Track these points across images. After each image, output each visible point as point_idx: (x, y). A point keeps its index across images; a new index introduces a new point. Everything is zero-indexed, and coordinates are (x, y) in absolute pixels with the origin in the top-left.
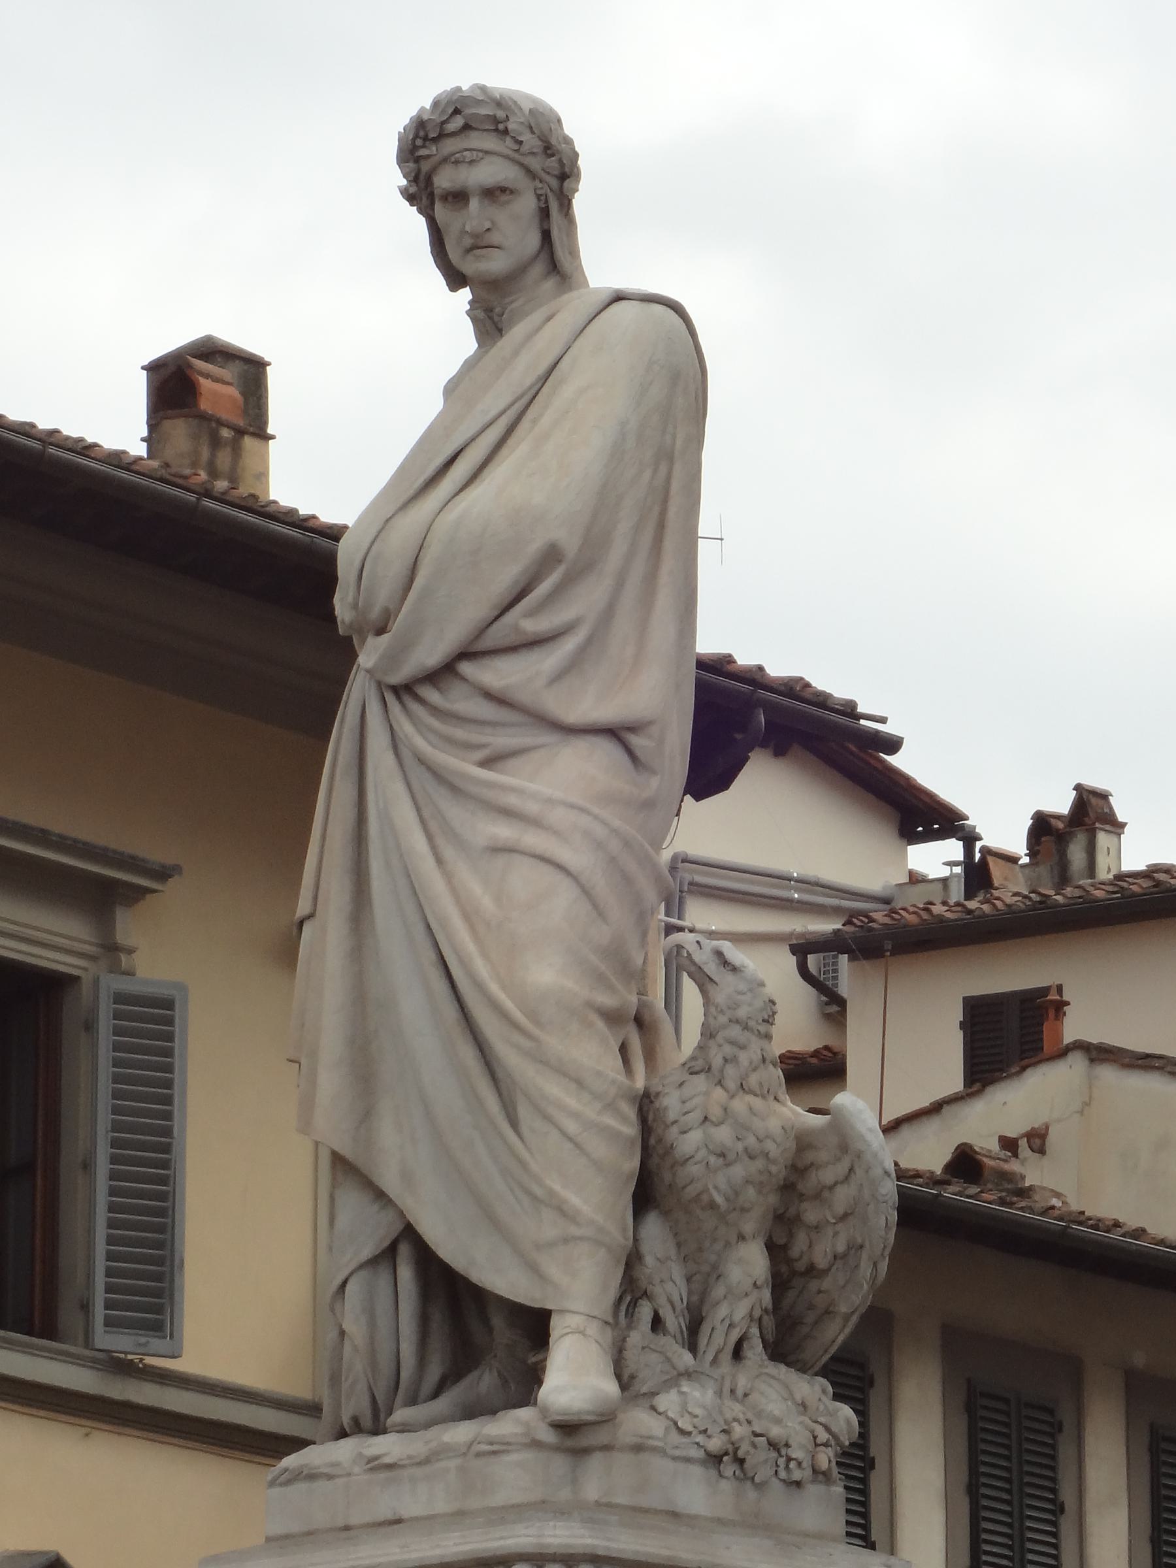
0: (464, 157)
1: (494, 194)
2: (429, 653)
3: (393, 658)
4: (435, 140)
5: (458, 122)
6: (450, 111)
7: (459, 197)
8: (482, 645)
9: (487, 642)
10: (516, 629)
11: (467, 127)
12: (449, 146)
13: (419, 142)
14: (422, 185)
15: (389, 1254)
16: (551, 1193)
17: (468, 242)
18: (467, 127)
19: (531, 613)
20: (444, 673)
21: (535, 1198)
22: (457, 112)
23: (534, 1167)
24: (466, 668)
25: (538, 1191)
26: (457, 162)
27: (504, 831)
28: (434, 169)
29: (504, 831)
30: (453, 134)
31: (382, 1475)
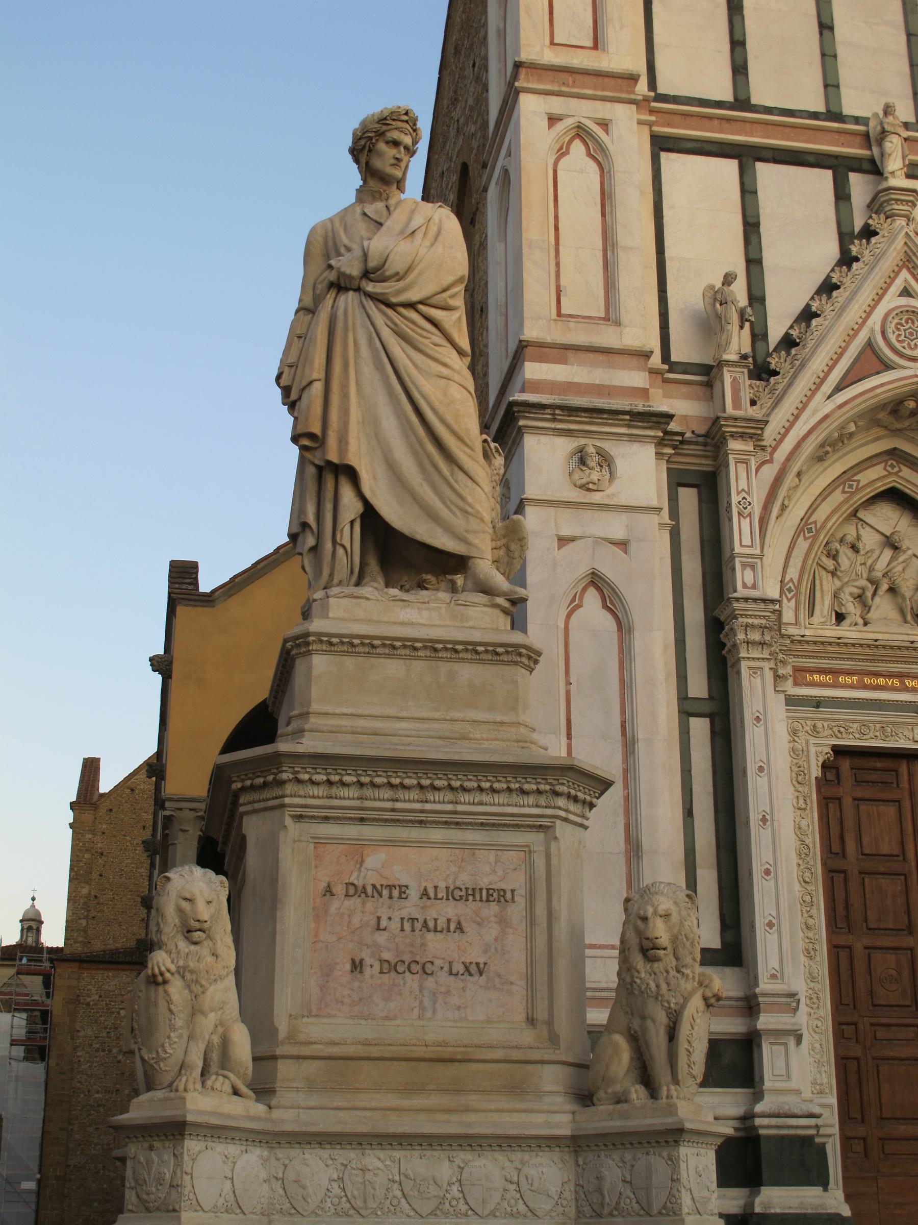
1: (406, 148)
3: (398, 292)
4: (394, 120)
5: (405, 118)
7: (396, 144)
8: (429, 301)
10: (445, 300)
11: (407, 122)
12: (400, 124)
16: (478, 512)
18: (407, 122)
19: (451, 297)
20: (411, 306)
21: (467, 512)
22: (406, 114)
23: (470, 499)
24: (421, 307)
25: (470, 510)
30: (403, 121)
31: (401, 603)
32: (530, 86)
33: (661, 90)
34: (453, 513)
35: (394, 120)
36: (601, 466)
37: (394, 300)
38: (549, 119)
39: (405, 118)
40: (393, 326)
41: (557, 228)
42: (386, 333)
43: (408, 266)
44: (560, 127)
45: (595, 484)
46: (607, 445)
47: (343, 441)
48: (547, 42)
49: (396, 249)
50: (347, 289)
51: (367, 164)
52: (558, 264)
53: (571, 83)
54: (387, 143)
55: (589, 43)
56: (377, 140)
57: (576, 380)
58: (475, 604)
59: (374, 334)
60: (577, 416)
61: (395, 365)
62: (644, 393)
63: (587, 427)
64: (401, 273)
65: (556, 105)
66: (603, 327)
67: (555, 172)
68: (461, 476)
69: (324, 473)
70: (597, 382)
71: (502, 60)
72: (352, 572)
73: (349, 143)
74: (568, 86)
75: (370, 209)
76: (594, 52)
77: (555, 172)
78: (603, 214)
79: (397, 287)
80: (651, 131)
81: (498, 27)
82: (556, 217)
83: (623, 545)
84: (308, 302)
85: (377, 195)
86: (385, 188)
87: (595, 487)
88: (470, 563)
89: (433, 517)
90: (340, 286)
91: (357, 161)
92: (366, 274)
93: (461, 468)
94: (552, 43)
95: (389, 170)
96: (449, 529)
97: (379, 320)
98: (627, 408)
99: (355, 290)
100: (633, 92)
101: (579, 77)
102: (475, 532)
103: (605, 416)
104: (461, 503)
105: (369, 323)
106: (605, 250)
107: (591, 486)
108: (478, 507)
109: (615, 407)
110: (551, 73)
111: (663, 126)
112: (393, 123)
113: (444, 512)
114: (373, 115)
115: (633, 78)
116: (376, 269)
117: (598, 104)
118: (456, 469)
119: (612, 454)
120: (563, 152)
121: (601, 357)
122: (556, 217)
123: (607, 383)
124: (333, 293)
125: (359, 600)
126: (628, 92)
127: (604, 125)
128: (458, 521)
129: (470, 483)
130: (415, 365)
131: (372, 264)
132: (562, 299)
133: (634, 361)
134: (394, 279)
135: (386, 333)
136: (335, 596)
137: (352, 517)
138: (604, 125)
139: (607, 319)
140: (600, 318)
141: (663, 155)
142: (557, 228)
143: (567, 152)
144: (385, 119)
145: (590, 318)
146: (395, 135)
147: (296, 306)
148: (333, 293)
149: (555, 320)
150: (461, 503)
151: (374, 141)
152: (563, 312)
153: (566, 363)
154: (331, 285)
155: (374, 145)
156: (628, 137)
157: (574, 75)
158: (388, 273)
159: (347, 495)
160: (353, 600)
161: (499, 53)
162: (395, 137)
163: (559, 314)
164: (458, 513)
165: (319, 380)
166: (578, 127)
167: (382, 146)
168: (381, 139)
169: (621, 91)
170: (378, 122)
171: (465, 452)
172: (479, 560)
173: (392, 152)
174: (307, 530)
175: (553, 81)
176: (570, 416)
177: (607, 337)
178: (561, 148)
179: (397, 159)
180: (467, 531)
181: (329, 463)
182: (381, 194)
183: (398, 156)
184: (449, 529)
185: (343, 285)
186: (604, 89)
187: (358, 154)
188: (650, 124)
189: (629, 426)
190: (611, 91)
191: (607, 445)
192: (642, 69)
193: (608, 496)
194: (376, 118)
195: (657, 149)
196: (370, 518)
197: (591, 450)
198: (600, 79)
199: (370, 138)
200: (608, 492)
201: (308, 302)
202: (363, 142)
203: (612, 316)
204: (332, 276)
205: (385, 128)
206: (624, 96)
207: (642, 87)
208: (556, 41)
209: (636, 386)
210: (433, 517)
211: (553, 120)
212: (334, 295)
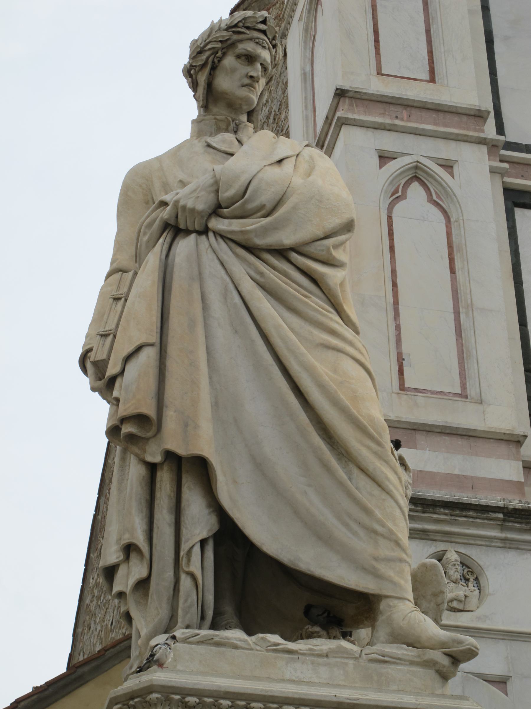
0: (263, 43)
2: (286, 238)
3: (265, 231)
4: (248, 28)
5: (262, 27)
6: (261, 20)
7: (250, 59)
9: (311, 249)
10: (328, 249)
11: (264, 32)
12: (256, 34)
13: (241, 24)
14: (225, 45)
15: (203, 543)
16: (391, 532)
17: (247, 81)
20: (282, 253)
21: (375, 532)
23: (378, 513)
26: (257, 43)
27: (334, 341)
28: (241, 41)
29: (334, 341)
32: (356, 117)
33: (511, 136)
34: (355, 534)
35: (248, 28)
36: (467, 580)
37: (259, 242)
38: (380, 157)
39: (262, 27)
40: (257, 277)
41: (395, 284)
42: (249, 287)
43: (280, 196)
44: (393, 166)
45: (460, 601)
46: (475, 554)
47: (188, 424)
48: (374, 71)
49: (260, 175)
50: (187, 232)
51: (209, 86)
52: (398, 327)
53: (405, 118)
54: (238, 57)
55: (426, 76)
56: (224, 54)
57: (430, 468)
58: (397, 660)
59: (231, 286)
60: (435, 513)
61: (262, 325)
62: (518, 487)
63: (447, 528)
64: (269, 206)
65: (389, 142)
66: (460, 403)
67: (390, 218)
68: (363, 481)
69: (159, 474)
70: (456, 472)
71: (310, 107)
72: (203, 617)
73: (184, 59)
74: (402, 119)
75: (217, 141)
76: (431, 85)
77: (390, 218)
78: (452, 271)
79: (263, 223)
80: (503, 182)
81: (303, 69)
82: (394, 271)
83: (501, 682)
84: (126, 261)
85: (223, 125)
86: (233, 116)
87: (461, 607)
88: (383, 606)
89: (324, 538)
90: (174, 229)
91: (194, 86)
92: (217, 210)
93: (363, 470)
94: (379, 73)
95: (243, 92)
96: (348, 556)
97: (239, 270)
98: (501, 504)
99: (200, 233)
100: (483, 131)
101: (414, 111)
102: (388, 560)
103: (471, 513)
104: (366, 520)
105: (223, 272)
106: (457, 314)
107: (455, 604)
108: (390, 524)
109: (483, 501)
110: (380, 105)
111: (517, 177)
112: (248, 32)
113: (340, 532)
114: (221, 20)
115: (479, 116)
116: (233, 202)
117: (441, 143)
118: (356, 471)
119: (481, 563)
120: (397, 196)
121: (460, 442)
122: (394, 271)
123: (469, 473)
124: (166, 237)
125: (222, 649)
126: (475, 130)
127: (448, 166)
128: (362, 546)
129: (377, 491)
130: (292, 330)
131: (226, 194)
132: (405, 369)
133: (503, 448)
134: (259, 214)
135: (249, 287)
136: (185, 640)
137: (204, 534)
138: (448, 166)
139: (463, 395)
140: (455, 394)
141: (519, 212)
142: (395, 284)
143: (403, 197)
144: (236, 26)
145: (442, 393)
146: (249, 47)
147: (106, 268)
148: (166, 237)
149: (398, 393)
150: (366, 520)
151: (219, 54)
152: (407, 385)
153: (415, 448)
154: (166, 226)
155: (220, 60)
156: (476, 183)
157: (409, 109)
158: (251, 206)
159: (195, 505)
160: (215, 649)
161: (306, 98)
162: (249, 49)
163: (402, 387)
164: (362, 533)
165: (152, 345)
166: (416, 167)
167: (229, 61)
168: (230, 53)
169: (468, 129)
170: (227, 30)
171: (368, 447)
172: (396, 602)
173: (244, 69)
174: (134, 557)
175: (384, 114)
176: (424, 512)
177: (465, 417)
178: (396, 191)
179: (251, 77)
180: (376, 559)
181: (170, 456)
182: (228, 125)
183: (252, 74)
184: (348, 556)
185: (182, 226)
186: (445, 126)
187: (197, 73)
188: (502, 173)
189: (503, 528)
190: (454, 127)
191: (475, 554)
192: (488, 105)
193: (479, 618)
194: (223, 26)
195: (510, 204)
196: (228, 537)
197: (452, 556)
198: (441, 115)
199: (215, 51)
200: (479, 612)
201: (126, 261)
202: (204, 57)
203: (472, 392)
204: (166, 213)
205: (235, 37)
206: (471, 133)
207: (490, 130)
208: (383, 72)
209: (507, 478)
210: (324, 538)
211: (384, 158)
212: (168, 240)
